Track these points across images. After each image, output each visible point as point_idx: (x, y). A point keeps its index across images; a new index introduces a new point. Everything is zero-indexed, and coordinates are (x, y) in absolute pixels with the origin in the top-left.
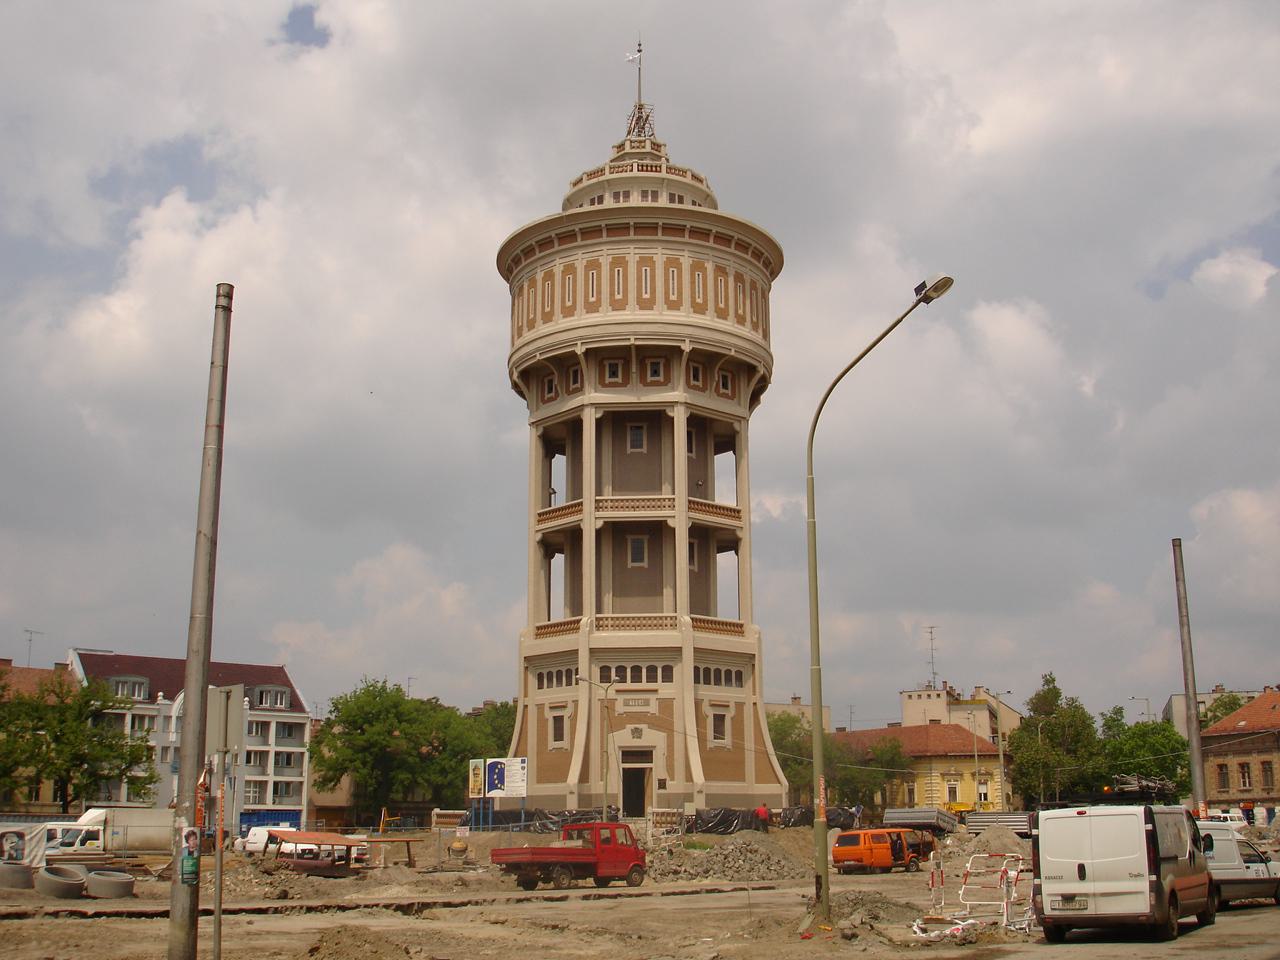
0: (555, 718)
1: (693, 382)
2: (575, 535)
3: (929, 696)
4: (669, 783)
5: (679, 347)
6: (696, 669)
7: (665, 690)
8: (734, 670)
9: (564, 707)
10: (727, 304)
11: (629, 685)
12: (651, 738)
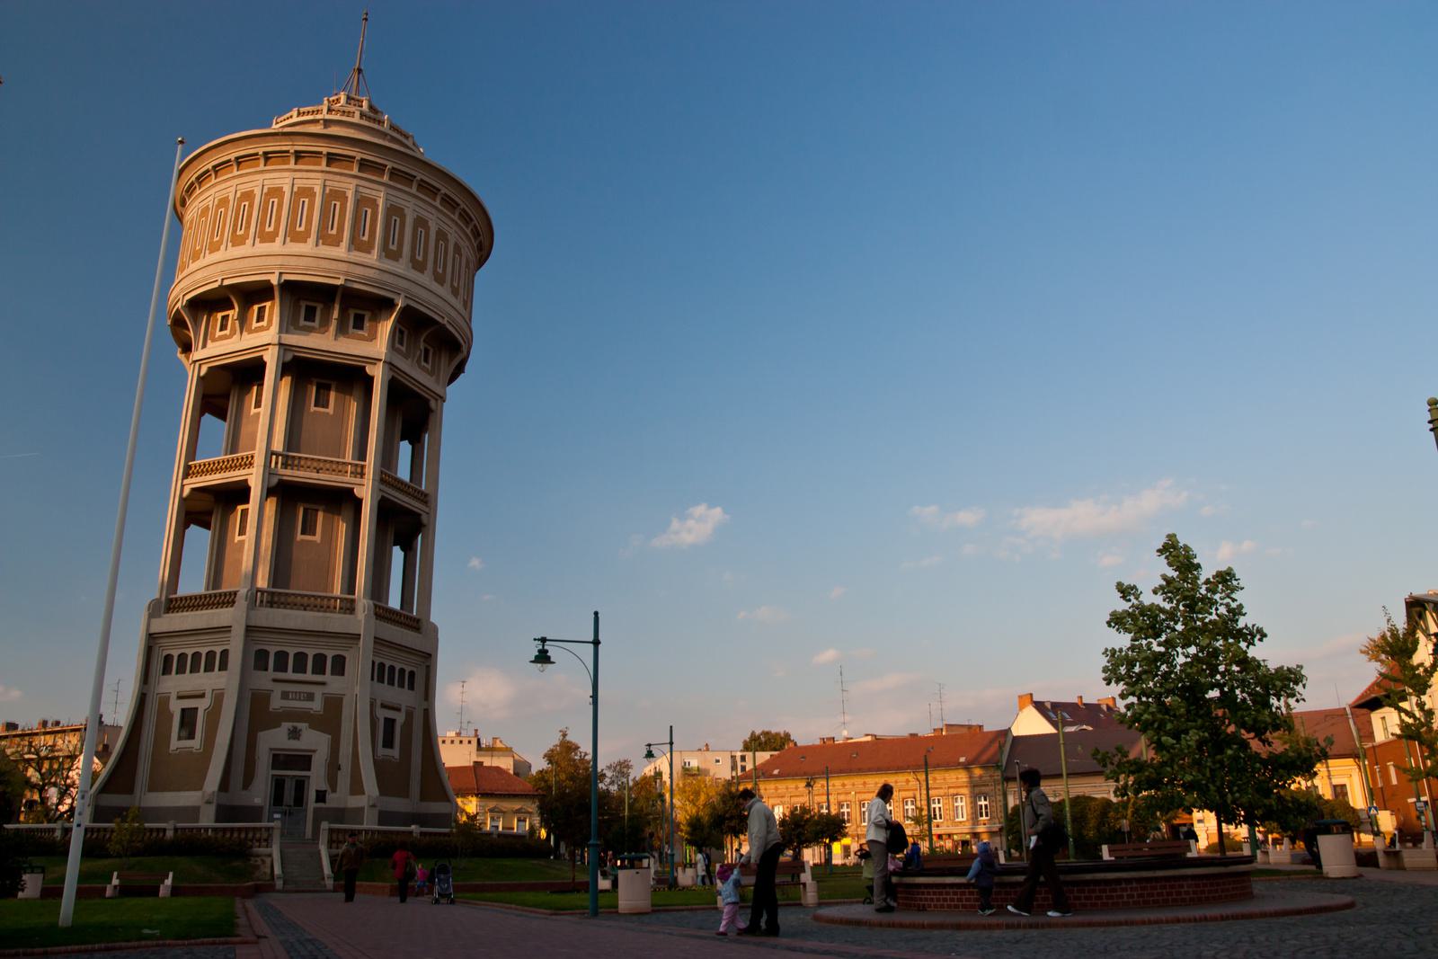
0: (183, 710)
1: (397, 345)
3: (461, 742)
4: (329, 796)
5: (392, 300)
6: (373, 663)
7: (334, 684)
8: (408, 669)
9: (202, 696)
10: (444, 270)
11: (290, 675)
12: (314, 741)
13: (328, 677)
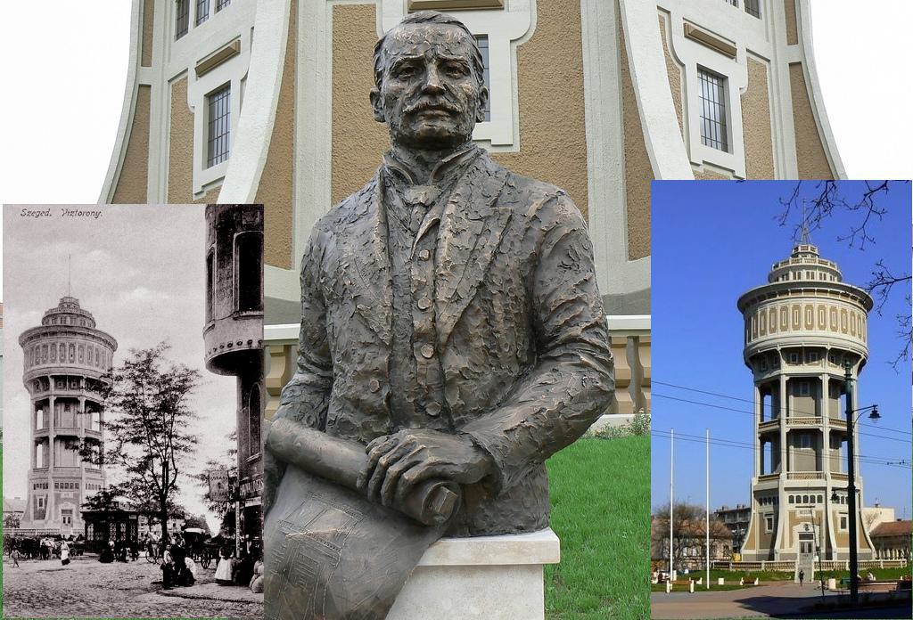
2: (777, 434)
13: (816, 504)
